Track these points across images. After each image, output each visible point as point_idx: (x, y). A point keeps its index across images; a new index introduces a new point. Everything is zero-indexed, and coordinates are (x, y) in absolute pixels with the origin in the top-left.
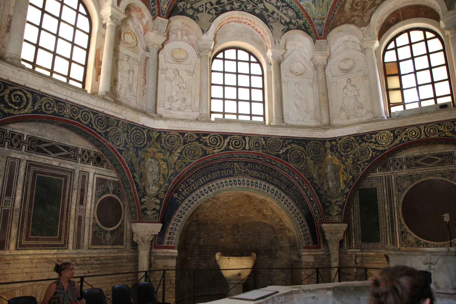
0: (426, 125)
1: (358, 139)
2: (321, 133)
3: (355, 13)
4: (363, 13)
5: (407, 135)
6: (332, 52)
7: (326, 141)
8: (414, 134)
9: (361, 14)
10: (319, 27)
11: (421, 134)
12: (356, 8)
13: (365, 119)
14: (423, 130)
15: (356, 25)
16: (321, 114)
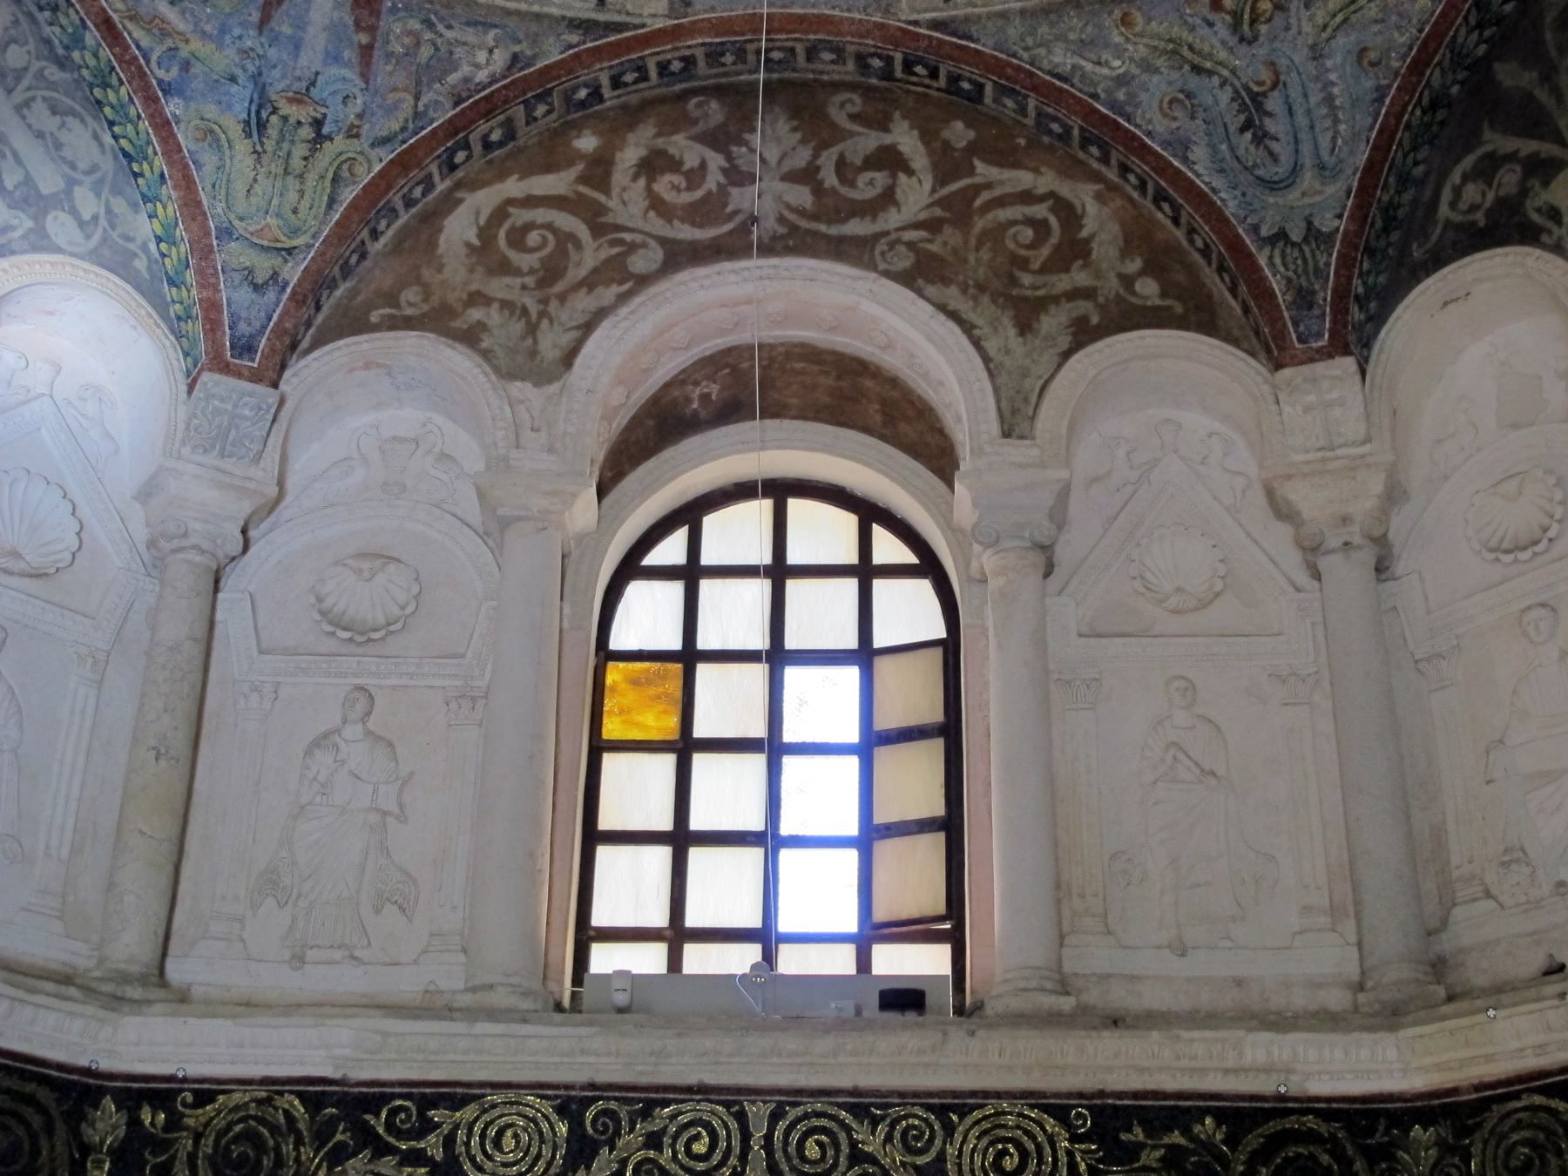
0: (785, 1099)
1: (332, 1123)
2: (78, 1025)
3: (499, 287)
4: (545, 301)
5: (659, 1148)
6: (292, 482)
7: (102, 1092)
8: (700, 1148)
9: (530, 302)
10: (244, 295)
11: (743, 1157)
12: (513, 255)
13: (406, 984)
14: (758, 1135)
15: (486, 355)
16: (111, 886)
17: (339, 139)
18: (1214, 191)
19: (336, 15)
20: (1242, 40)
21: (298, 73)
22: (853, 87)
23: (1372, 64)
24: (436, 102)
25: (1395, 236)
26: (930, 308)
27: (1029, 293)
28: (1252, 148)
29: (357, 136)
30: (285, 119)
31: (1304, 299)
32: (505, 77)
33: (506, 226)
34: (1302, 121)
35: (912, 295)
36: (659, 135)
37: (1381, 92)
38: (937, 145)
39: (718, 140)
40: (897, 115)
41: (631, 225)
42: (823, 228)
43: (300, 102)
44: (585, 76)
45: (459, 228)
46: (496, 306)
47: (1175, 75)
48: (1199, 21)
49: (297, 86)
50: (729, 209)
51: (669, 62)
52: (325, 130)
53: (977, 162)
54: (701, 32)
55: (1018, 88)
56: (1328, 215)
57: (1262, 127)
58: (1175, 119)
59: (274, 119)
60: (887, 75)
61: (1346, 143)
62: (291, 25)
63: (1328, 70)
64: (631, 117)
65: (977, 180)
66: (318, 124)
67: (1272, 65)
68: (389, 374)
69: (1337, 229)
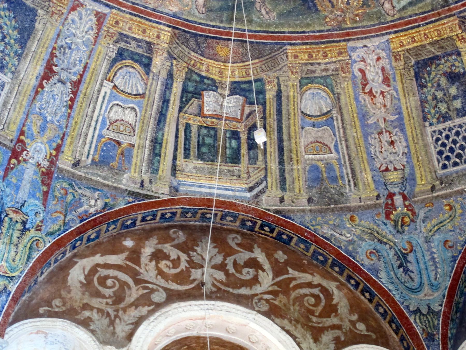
3: (96, 302)
4: (117, 311)
12: (100, 288)
15: (93, 332)
17: (33, 231)
18: (390, 291)
19: (35, 177)
20: (398, 232)
21: (17, 200)
22: (237, 232)
23: (450, 247)
24: (73, 219)
25: (458, 314)
26: (279, 328)
27: (316, 325)
28: (403, 275)
29: (40, 230)
30: (11, 219)
31: (430, 337)
32: (101, 212)
33: (97, 276)
34: (422, 266)
35: (271, 322)
36: (159, 243)
37: (454, 258)
38: (272, 260)
39: (184, 248)
40: (256, 246)
41: (151, 281)
42: (231, 290)
43: (17, 213)
44: (133, 215)
45: (76, 275)
46: (95, 311)
47: (372, 243)
48: (381, 223)
49: (16, 205)
50: (191, 278)
51: (166, 213)
52: (27, 226)
53: (289, 269)
54: (182, 203)
55: (308, 241)
56: (436, 305)
57: (406, 267)
58: (372, 260)
59: (6, 219)
60: (252, 229)
61: (441, 277)
62: (16, 179)
63: (432, 248)
64: (147, 234)
65: (290, 276)
66: (24, 223)
67: (410, 243)
68: (45, 337)
69: (441, 310)
